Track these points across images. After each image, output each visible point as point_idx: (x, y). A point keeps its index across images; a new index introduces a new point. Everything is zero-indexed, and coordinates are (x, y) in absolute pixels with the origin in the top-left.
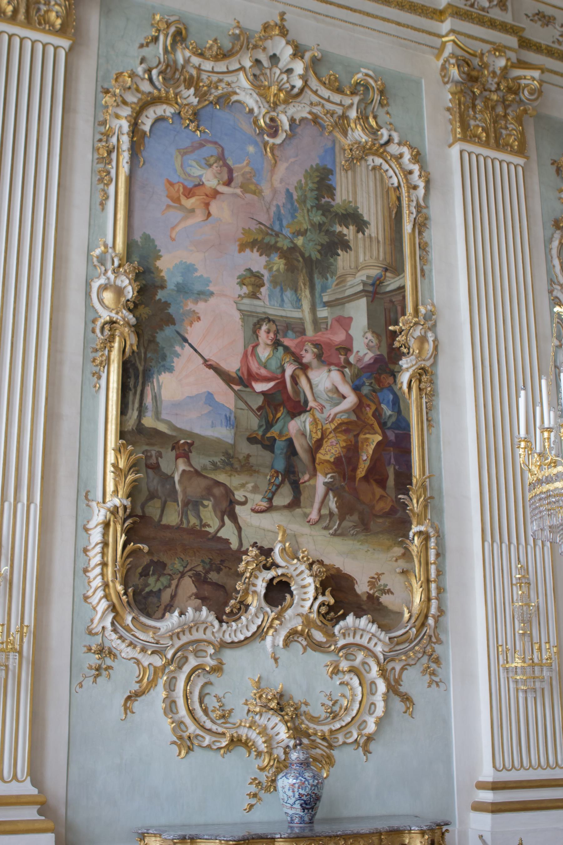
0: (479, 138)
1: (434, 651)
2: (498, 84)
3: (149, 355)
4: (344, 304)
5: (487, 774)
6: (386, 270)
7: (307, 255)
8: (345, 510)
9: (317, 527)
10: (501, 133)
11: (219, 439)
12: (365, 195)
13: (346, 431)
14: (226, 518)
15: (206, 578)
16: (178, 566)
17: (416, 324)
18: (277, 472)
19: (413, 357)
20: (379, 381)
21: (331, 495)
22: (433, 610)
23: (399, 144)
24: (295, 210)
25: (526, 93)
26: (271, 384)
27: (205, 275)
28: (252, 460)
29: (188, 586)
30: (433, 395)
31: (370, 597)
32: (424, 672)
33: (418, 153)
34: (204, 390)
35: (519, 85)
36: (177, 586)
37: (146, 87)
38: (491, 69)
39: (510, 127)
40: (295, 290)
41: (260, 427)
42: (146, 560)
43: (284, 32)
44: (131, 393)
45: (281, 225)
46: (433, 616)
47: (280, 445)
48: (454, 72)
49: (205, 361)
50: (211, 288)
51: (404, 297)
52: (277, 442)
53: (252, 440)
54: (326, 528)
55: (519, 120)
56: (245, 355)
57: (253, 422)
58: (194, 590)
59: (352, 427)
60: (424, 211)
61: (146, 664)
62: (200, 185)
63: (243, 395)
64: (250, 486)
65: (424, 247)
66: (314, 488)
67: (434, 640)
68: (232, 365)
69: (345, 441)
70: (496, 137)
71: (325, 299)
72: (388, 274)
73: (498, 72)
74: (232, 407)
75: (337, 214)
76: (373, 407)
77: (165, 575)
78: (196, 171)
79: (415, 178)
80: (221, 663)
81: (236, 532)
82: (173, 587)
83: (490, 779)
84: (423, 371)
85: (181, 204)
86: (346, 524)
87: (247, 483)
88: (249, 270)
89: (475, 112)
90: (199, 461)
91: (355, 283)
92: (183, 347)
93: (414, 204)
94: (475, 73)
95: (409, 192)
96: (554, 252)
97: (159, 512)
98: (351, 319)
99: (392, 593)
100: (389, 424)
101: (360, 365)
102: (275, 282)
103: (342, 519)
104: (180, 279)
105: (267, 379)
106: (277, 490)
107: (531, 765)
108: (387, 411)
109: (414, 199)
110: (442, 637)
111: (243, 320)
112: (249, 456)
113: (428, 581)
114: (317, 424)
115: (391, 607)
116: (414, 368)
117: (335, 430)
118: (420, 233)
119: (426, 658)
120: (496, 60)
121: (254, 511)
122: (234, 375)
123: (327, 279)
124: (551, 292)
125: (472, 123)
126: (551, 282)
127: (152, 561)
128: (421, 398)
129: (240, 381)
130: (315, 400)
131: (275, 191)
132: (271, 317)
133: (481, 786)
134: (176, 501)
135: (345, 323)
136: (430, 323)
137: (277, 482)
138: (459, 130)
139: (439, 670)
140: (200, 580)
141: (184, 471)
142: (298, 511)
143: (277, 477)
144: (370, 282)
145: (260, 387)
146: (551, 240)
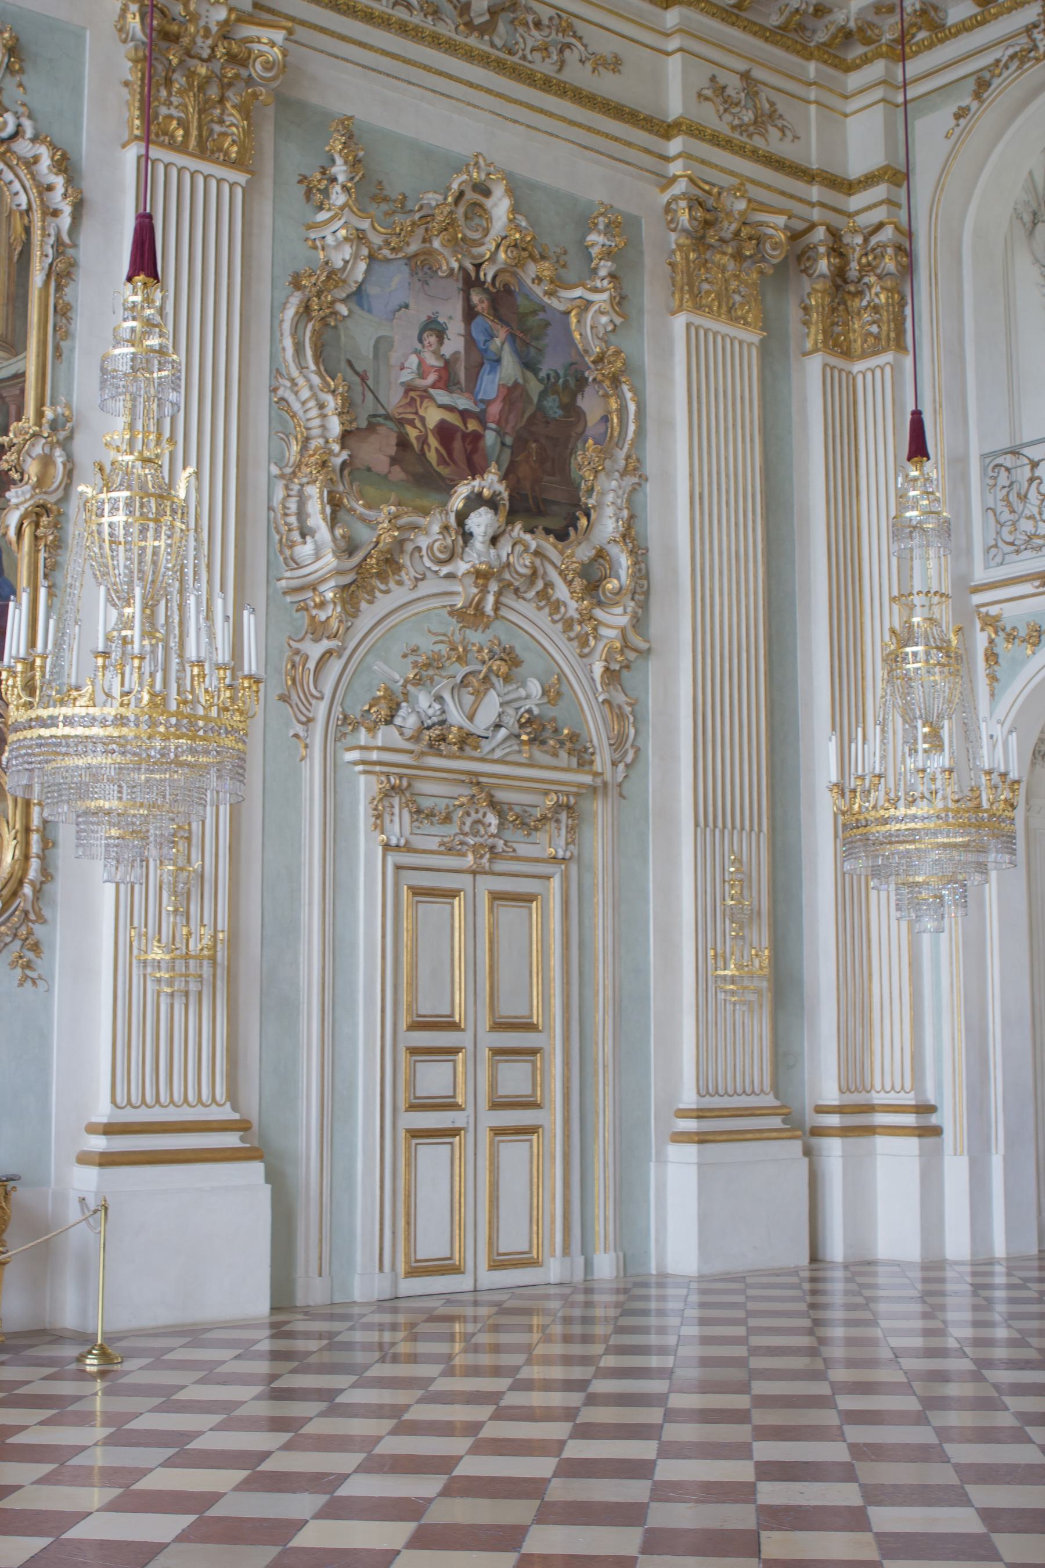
0: (172, 137)
1: (30, 933)
2: (213, 48)
5: (103, 1112)
10: (211, 131)
17: (35, 435)
19: (28, 488)
22: (32, 873)
23: (34, 140)
25: (258, 66)
30: (58, 545)
32: (13, 965)
33: (64, 157)
35: (250, 51)
38: (202, 23)
39: (228, 120)
46: (32, 883)
48: (134, 23)
51: (23, 391)
55: (245, 110)
60: (70, 251)
65: (64, 311)
67: (32, 917)
70: (200, 135)
73: (214, 29)
79: (57, 198)
83: (105, 1120)
84: (41, 510)
89: (170, 94)
93: (52, 240)
94: (175, 28)
95: (43, 221)
96: (287, 326)
107: (172, 1101)
109: (52, 232)
110: (46, 913)
113: (27, 830)
116: (26, 505)
118: (59, 288)
119: (18, 943)
120: (212, 9)
124: (274, 390)
125: (163, 111)
126: (277, 372)
128: (38, 551)
133: (92, 1129)
136: (62, 435)
138: (137, 122)
139: (39, 961)
146: (284, 306)
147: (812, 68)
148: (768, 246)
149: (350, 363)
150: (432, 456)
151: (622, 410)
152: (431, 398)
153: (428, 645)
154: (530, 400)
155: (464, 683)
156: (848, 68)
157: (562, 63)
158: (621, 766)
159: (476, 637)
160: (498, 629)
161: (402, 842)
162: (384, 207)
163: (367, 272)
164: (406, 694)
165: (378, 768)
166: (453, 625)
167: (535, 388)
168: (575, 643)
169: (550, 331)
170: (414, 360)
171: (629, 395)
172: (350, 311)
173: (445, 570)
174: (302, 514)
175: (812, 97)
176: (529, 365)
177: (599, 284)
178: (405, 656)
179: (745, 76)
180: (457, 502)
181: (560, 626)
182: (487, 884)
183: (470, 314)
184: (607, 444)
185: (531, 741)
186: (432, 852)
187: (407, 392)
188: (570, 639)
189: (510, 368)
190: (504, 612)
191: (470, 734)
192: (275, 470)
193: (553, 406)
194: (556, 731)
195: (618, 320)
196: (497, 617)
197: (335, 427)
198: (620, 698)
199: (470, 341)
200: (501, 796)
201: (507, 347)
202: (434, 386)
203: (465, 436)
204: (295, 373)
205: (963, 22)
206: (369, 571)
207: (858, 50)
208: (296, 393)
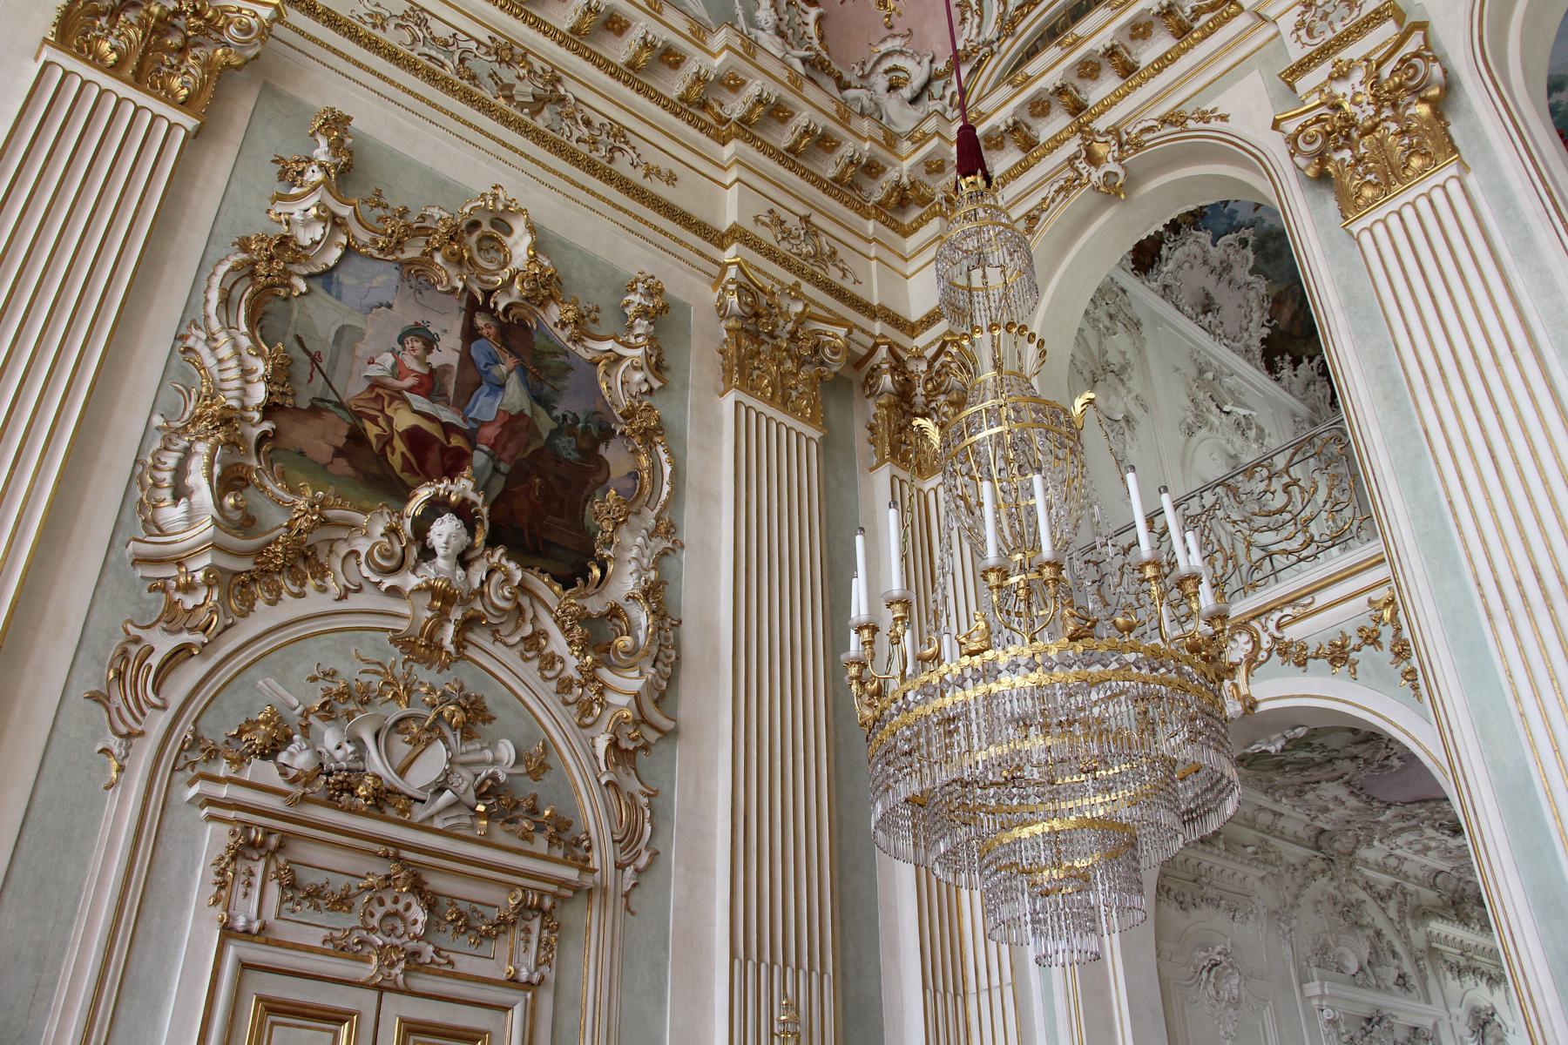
124: (180, 337)
147: (871, 226)
148: (827, 351)
149: (299, 340)
150: (396, 461)
151: (655, 468)
152: (406, 401)
153: (350, 672)
154: (539, 436)
155: (399, 725)
156: (906, 235)
157: (611, 160)
158: (630, 870)
159: (425, 676)
160: (463, 672)
161: (256, 926)
162: (380, 212)
163: (341, 259)
164: (306, 729)
165: (232, 814)
166: (395, 655)
167: (545, 424)
168: (574, 709)
169: (571, 375)
170: (389, 359)
171: (664, 457)
172: (310, 290)
173: (388, 582)
174: (180, 471)
175: (872, 254)
176: (538, 399)
177: (632, 340)
178: (314, 679)
179: (805, 220)
180: (415, 507)
181: (553, 685)
182: (398, 1008)
183: (470, 334)
184: (635, 495)
185: (487, 815)
186: (310, 949)
187: (372, 387)
188: (566, 703)
189: (515, 396)
190: (471, 652)
191: (393, 792)
192: (158, 421)
193: (566, 446)
194: (534, 811)
195: (656, 384)
196: (462, 657)
197: (259, 393)
198: (634, 785)
199: (466, 359)
200: (436, 882)
201: (514, 376)
202: (411, 389)
203: (444, 450)
204: (215, 324)
205: (1008, 172)
206: (269, 565)
207: (915, 213)
208: (213, 350)
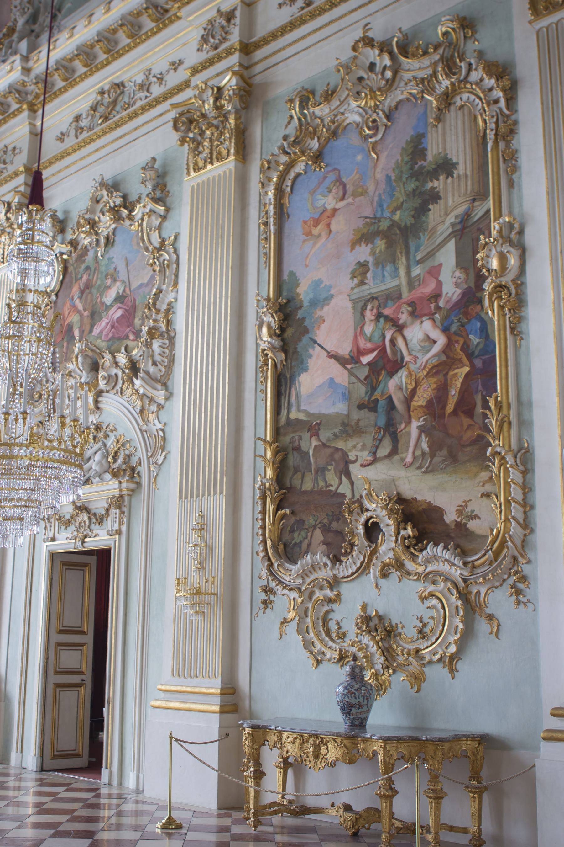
3: (293, 364)
4: (434, 254)
6: (474, 200)
7: (403, 225)
8: (435, 447)
9: (411, 469)
11: (337, 413)
12: (454, 137)
13: (436, 373)
14: (343, 477)
15: (329, 528)
16: (311, 521)
18: (380, 428)
20: (466, 314)
21: (423, 436)
24: (393, 190)
26: (375, 353)
27: (328, 284)
28: (361, 424)
29: (318, 535)
31: (458, 525)
34: (328, 377)
36: (311, 536)
37: (284, 159)
40: (394, 261)
41: (366, 393)
42: (293, 520)
43: (369, 42)
44: (283, 397)
45: (382, 210)
47: (382, 403)
49: (328, 353)
50: (332, 292)
52: (380, 402)
53: (361, 407)
54: (419, 468)
56: (356, 337)
57: (361, 390)
58: (322, 539)
59: (442, 368)
61: (292, 598)
62: (325, 210)
63: (354, 371)
64: (359, 446)
66: (409, 434)
68: (345, 350)
69: (435, 383)
71: (418, 258)
72: (476, 204)
74: (346, 384)
75: (428, 172)
76: (461, 341)
77: (303, 529)
78: (320, 203)
80: (338, 596)
81: (350, 487)
82: (309, 538)
85: (312, 235)
86: (437, 459)
87: (357, 444)
88: (359, 263)
90: (325, 435)
91: (445, 229)
92: (313, 348)
97: (300, 481)
98: (441, 265)
99: (479, 518)
100: (477, 353)
101: (449, 306)
102: (377, 264)
103: (433, 456)
104: (311, 296)
105: (371, 351)
106: (379, 443)
108: (474, 339)
110: (531, 556)
111: (354, 308)
112: (359, 420)
114: (411, 375)
115: (478, 532)
117: (426, 376)
121: (363, 466)
122: (348, 357)
123: (420, 238)
127: (296, 520)
129: (348, 361)
130: (410, 354)
131: (377, 183)
132: (374, 296)
134: (311, 471)
135: (434, 272)
137: (380, 437)
139: (527, 590)
140: (326, 529)
141: (316, 446)
142: (397, 458)
143: (380, 432)
144: (459, 220)
145: (365, 360)
